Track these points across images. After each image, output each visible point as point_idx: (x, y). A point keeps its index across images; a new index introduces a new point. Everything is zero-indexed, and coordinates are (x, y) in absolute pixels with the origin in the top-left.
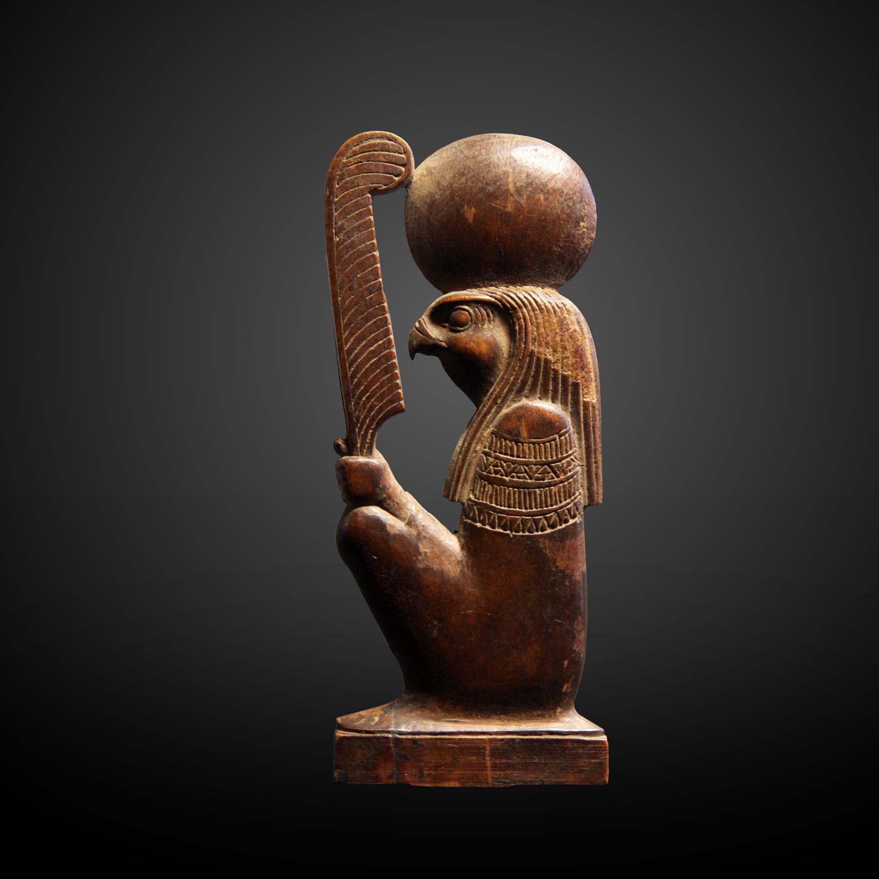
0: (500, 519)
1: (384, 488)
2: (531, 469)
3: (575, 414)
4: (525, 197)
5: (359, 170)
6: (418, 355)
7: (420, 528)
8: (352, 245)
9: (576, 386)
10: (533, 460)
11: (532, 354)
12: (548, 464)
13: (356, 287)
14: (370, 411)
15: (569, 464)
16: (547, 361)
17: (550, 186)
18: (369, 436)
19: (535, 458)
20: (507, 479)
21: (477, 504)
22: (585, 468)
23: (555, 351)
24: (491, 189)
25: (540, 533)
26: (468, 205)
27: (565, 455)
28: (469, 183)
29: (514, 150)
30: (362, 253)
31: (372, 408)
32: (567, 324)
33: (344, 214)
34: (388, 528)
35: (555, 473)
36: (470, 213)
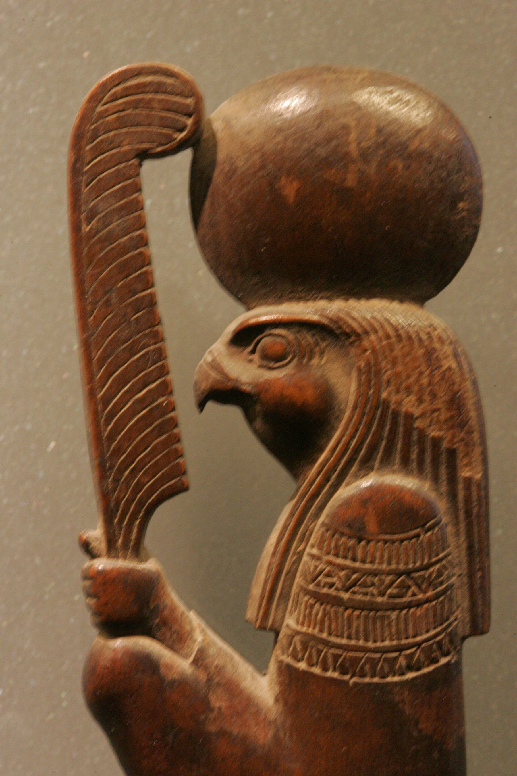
0: (336, 657)
1: (157, 610)
2: (382, 582)
3: (452, 495)
4: (374, 164)
5: (122, 123)
6: (210, 405)
7: (212, 669)
8: (110, 238)
9: (452, 453)
10: (384, 566)
11: (386, 404)
12: (408, 573)
13: (114, 300)
14: (136, 491)
15: (440, 573)
16: (409, 417)
17: (412, 147)
18: (135, 531)
19: (389, 563)
20: (346, 596)
21: (298, 633)
22: (465, 580)
23: (420, 401)
24: (322, 152)
25: (396, 679)
26: (288, 176)
27: (434, 560)
28: (289, 143)
29: (358, 92)
30: (125, 249)
31: (139, 486)
32: (438, 359)
33: (99, 190)
34: (162, 670)
35: (419, 586)
36: (290, 189)
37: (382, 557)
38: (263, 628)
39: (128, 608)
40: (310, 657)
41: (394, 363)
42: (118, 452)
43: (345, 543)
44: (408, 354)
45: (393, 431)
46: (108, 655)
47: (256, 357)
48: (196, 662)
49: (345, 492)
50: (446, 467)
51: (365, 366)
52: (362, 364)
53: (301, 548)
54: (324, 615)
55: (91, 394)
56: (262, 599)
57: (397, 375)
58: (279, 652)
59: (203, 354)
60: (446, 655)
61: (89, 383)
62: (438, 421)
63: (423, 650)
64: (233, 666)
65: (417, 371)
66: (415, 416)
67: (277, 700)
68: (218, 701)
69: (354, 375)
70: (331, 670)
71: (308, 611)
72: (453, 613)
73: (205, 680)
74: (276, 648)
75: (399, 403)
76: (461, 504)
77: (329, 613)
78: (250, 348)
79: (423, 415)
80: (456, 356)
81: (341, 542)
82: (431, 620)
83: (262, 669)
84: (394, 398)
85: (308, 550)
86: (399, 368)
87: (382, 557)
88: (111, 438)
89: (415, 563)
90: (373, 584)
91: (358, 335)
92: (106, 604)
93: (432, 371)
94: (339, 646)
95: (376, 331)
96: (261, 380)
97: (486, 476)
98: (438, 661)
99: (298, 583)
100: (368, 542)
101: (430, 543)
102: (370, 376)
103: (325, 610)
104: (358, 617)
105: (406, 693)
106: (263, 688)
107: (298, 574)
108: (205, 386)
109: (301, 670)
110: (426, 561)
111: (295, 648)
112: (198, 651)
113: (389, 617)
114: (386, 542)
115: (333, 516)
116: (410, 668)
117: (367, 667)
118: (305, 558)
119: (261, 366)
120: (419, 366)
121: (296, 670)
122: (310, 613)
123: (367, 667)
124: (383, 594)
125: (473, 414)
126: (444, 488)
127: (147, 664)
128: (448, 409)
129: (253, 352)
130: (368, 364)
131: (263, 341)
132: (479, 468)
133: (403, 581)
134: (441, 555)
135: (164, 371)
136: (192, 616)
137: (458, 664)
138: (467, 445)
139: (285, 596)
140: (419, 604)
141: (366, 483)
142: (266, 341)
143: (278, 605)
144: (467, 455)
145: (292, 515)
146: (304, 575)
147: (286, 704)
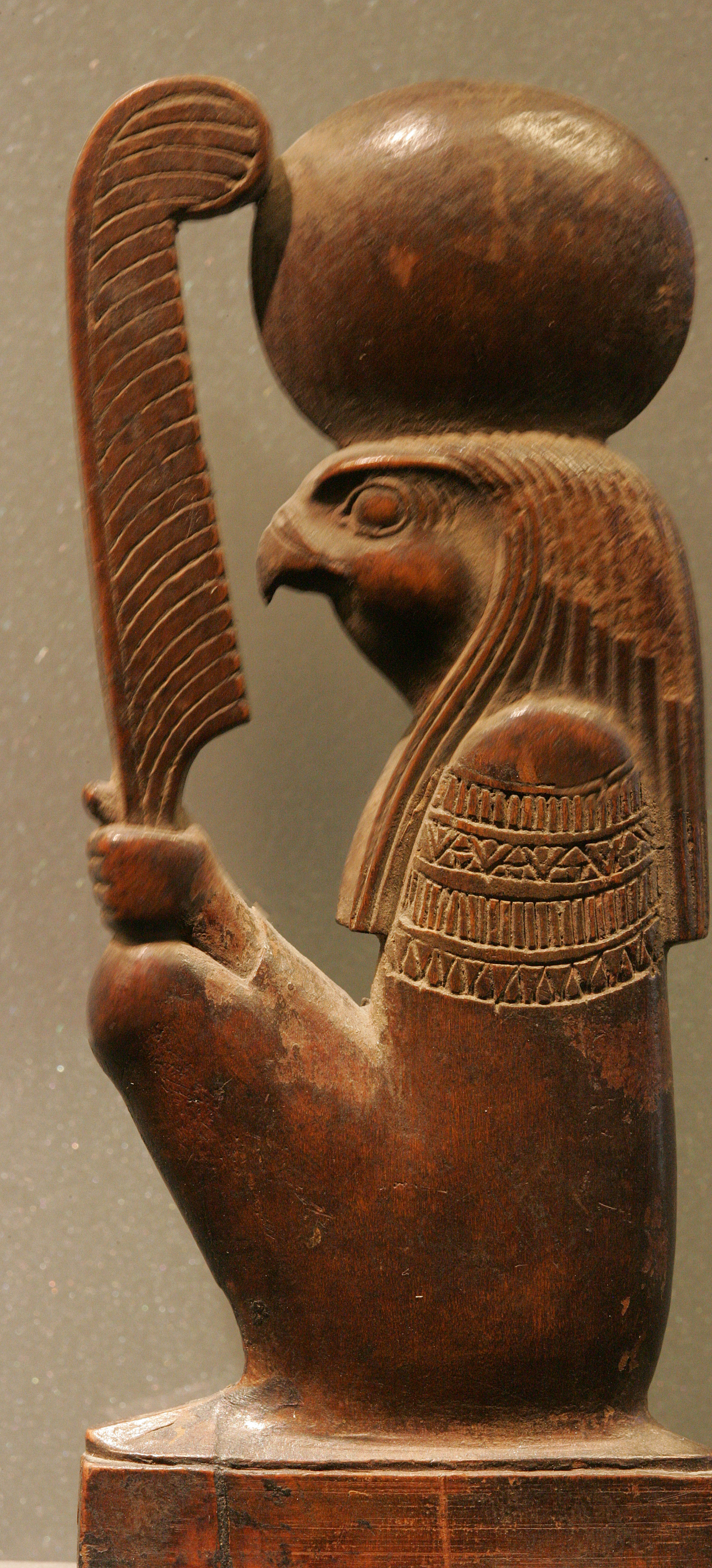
0: (473, 971)
2: (542, 855)
3: (649, 729)
6: (281, 593)
7: (284, 992)
9: (648, 665)
11: (549, 590)
12: (582, 844)
14: (169, 722)
16: (584, 611)
21: (415, 934)
23: (600, 586)
25: (566, 1003)
31: (174, 715)
37: (542, 818)
38: (361, 930)
39: (158, 899)
40: (434, 970)
41: (561, 528)
42: (142, 664)
43: (487, 798)
44: (582, 515)
45: (560, 632)
46: (128, 970)
47: (351, 519)
48: (259, 981)
49: (487, 724)
50: (640, 686)
51: (517, 533)
52: (513, 530)
53: (420, 806)
54: (456, 905)
55: (102, 575)
56: (360, 886)
57: (566, 547)
58: (387, 966)
59: (271, 516)
60: (640, 969)
61: (98, 560)
62: (628, 617)
63: (607, 961)
64: (316, 986)
65: (596, 541)
66: (593, 610)
67: (383, 1038)
68: (293, 1039)
69: (501, 546)
70: (466, 991)
71: (429, 903)
72: (651, 904)
73: (273, 1006)
74: (382, 960)
75: (569, 590)
76: (662, 743)
77: (464, 903)
78: (343, 506)
79: (604, 608)
80: (655, 518)
81: (479, 797)
82: (619, 913)
83: (360, 996)
84: (561, 583)
85: (430, 809)
86: (569, 537)
87: (542, 818)
88: (132, 641)
89: (592, 828)
90: (530, 860)
91: (506, 487)
92: (124, 893)
93: (619, 541)
94: (479, 955)
95: (534, 481)
96: (359, 555)
97: (699, 699)
98: (629, 977)
99: (415, 859)
100: (521, 795)
101: (615, 798)
102: (525, 548)
103: (456, 899)
104: (507, 909)
105: (581, 1025)
106: (363, 1022)
107: (415, 847)
108: (274, 563)
109: (420, 988)
110: (609, 825)
111: (411, 958)
112: (263, 963)
113: (554, 908)
114: (547, 796)
115: (470, 758)
116: (586, 987)
117: (521, 986)
118: (426, 821)
119: (359, 534)
120: (599, 534)
121: (414, 989)
122: (434, 905)
123: (521, 986)
124: (543, 877)
125: (680, 606)
126: (636, 718)
127: (187, 982)
128: (643, 599)
129: (347, 512)
130: (521, 530)
131: (362, 495)
132: (690, 688)
133: (575, 855)
134: (632, 817)
135: (211, 541)
136: (255, 912)
137: (661, 982)
138: (671, 653)
139: (395, 882)
140: (599, 891)
141: (518, 711)
142: (367, 496)
143: (384, 894)
144: (671, 668)
145: (406, 759)
146: (424, 848)
147: (397, 1043)
